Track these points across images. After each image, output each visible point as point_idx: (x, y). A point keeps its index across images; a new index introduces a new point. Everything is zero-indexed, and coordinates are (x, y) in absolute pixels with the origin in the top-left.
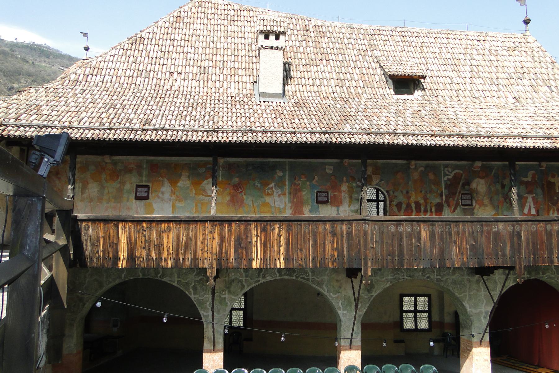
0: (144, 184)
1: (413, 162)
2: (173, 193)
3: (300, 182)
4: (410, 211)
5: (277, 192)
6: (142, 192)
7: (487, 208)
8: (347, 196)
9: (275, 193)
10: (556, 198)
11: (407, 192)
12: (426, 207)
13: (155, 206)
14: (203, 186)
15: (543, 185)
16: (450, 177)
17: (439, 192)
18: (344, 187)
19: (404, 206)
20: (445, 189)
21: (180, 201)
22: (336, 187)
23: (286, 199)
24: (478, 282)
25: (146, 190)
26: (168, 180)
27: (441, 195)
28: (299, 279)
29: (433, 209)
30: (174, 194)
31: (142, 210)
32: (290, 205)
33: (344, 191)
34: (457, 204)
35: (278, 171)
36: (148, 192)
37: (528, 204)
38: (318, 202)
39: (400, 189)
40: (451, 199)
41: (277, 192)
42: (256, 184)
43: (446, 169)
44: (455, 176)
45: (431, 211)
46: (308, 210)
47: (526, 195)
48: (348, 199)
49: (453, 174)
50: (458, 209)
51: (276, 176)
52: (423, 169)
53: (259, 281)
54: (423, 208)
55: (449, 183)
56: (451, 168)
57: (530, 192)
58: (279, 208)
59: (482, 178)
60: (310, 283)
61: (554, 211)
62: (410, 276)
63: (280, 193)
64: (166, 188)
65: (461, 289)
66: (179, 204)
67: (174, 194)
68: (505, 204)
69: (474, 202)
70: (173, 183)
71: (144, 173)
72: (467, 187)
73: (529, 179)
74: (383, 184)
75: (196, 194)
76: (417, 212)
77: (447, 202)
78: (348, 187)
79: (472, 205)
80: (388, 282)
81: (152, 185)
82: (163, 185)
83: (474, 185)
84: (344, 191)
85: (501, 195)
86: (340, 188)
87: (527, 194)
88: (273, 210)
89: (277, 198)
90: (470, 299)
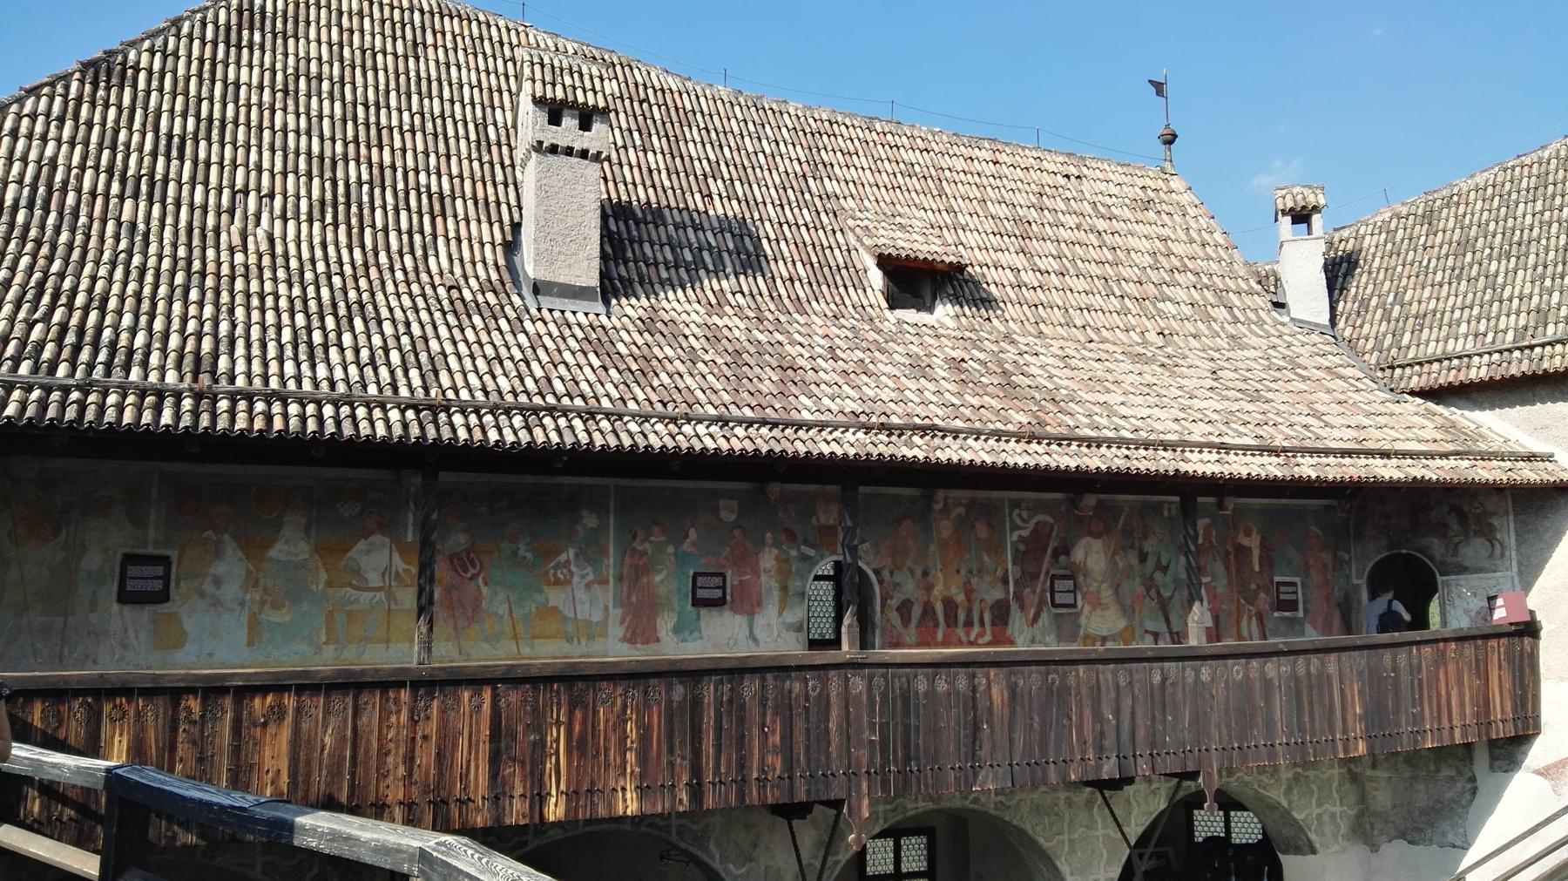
0: (151, 550)
1: (941, 494)
2: (252, 582)
3: (647, 545)
4: (931, 624)
5: (583, 577)
6: (144, 579)
8: (773, 583)
9: (576, 579)
10: (1253, 586)
11: (925, 574)
12: (969, 611)
13: (189, 624)
14: (354, 560)
15: (1227, 553)
16: (1025, 533)
17: (1000, 573)
18: (768, 560)
19: (917, 611)
20: (1014, 563)
21: (277, 605)
22: (745, 559)
23: (607, 595)
24: (1089, 803)
25: (160, 570)
26: (235, 538)
27: (1005, 581)
28: (643, 829)
29: (987, 617)
30: (256, 584)
31: (143, 636)
32: (619, 611)
33: (766, 572)
34: (1042, 602)
35: (584, 513)
36: (166, 579)
38: (698, 603)
39: (909, 563)
40: (1028, 590)
41: (580, 575)
42: (522, 552)
43: (1017, 511)
44: (1035, 531)
45: (982, 624)
46: (670, 625)
48: (776, 593)
49: (1031, 525)
50: (1044, 615)
51: (579, 528)
52: (961, 510)
53: (525, 843)
54: (962, 616)
55: (1022, 547)
56: (1027, 509)
58: (589, 623)
59: (1096, 536)
60: (674, 838)
61: (1250, 618)
62: (932, 800)
63: (591, 577)
64: (231, 566)
65: (1051, 826)
66: (272, 616)
67: (256, 584)
68: (1147, 600)
69: (1079, 597)
70: (254, 548)
71: (153, 517)
72: (1062, 558)
74: (866, 552)
75: (329, 584)
76: (948, 626)
77: (1018, 596)
78: (777, 558)
79: (1074, 606)
80: (877, 820)
81: (181, 556)
82: (218, 555)
83: (1078, 555)
84: (766, 572)
86: (757, 561)
88: (570, 628)
89: (581, 595)
90: (1072, 851)
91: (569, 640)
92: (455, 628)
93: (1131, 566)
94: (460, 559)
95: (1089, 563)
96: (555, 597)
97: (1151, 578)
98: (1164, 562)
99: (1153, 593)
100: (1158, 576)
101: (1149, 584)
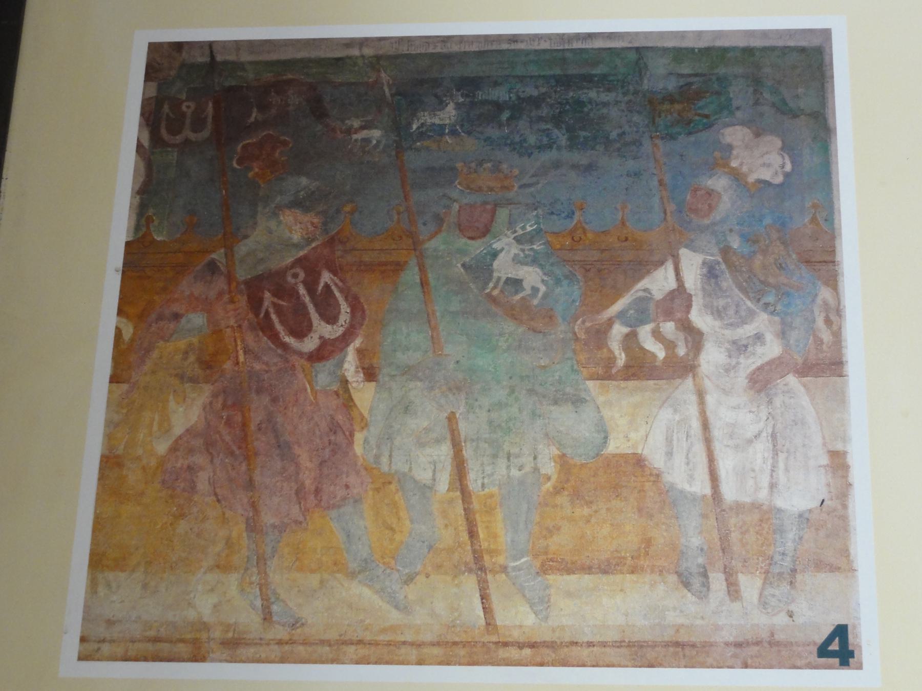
5: (740, 348)
9: (712, 357)
58: (766, 517)
63: (772, 349)
89: (733, 411)
91: (690, 580)
92: (253, 527)
94: (283, 291)
96: (645, 426)
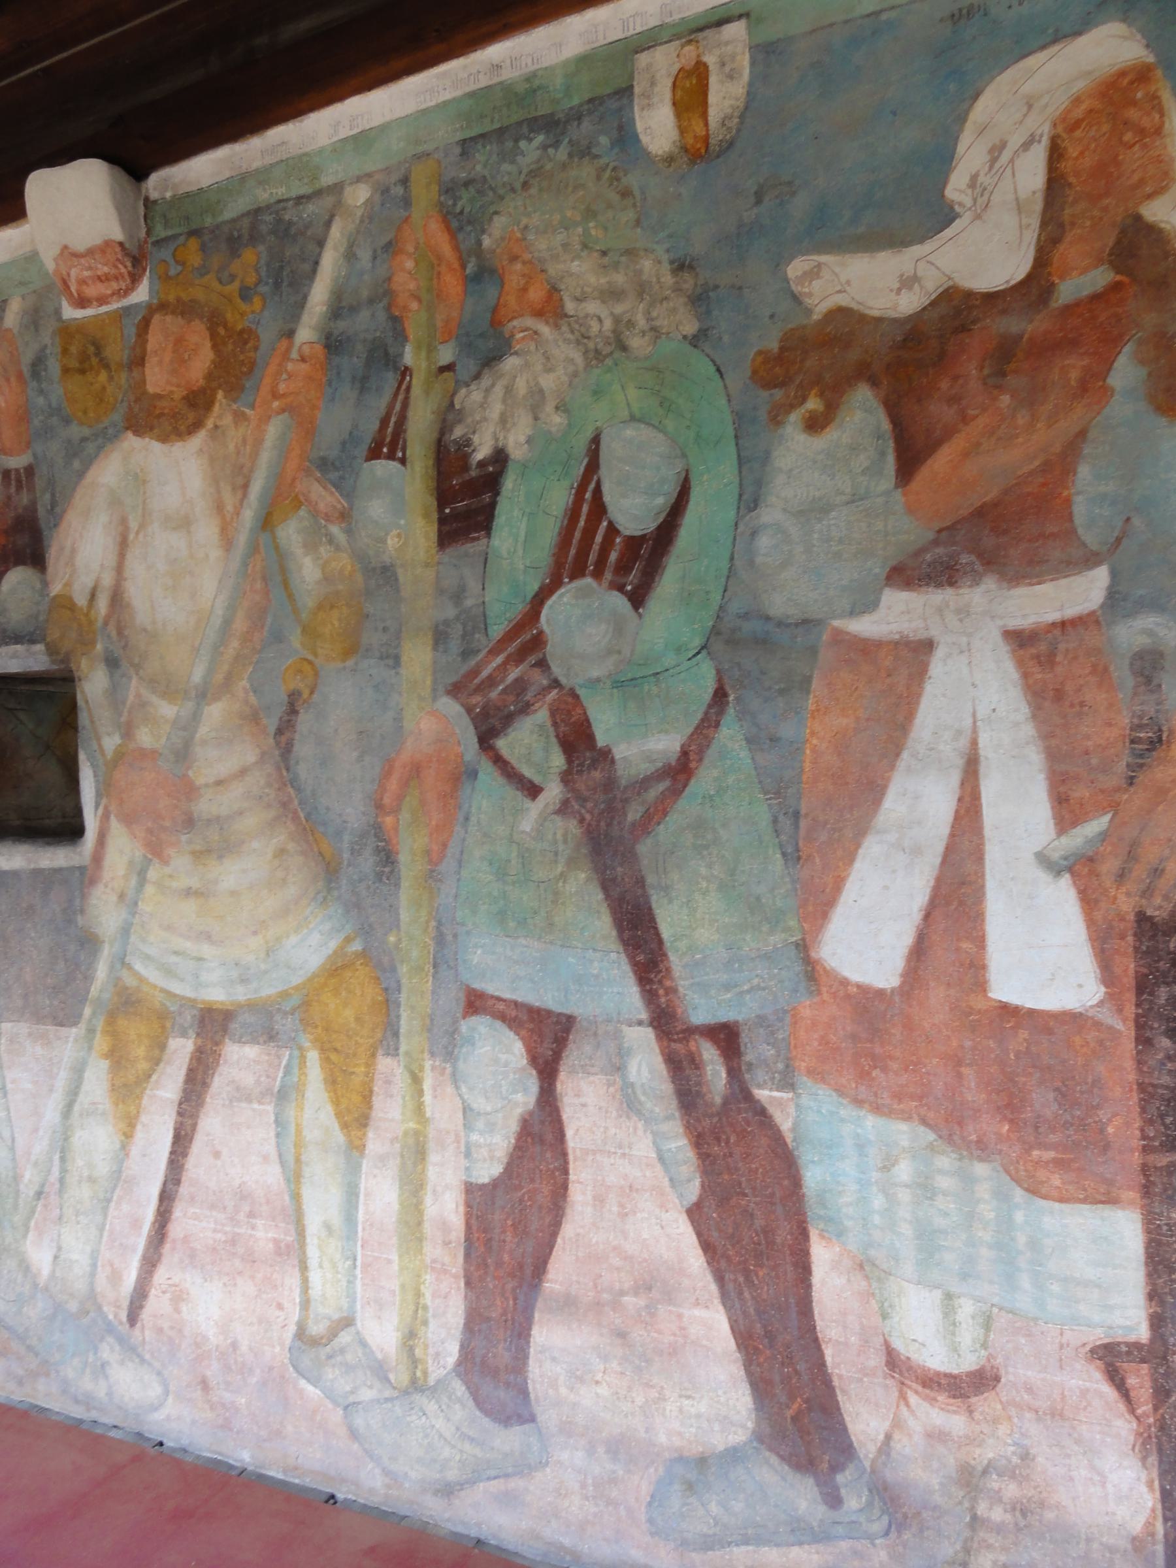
7: (231, 874)
37: (918, 802)
47: (897, 614)
57: (998, 535)
68: (488, 793)
73: (988, 250)
85: (418, 658)
87: (923, 570)
93: (383, 575)
95: (135, 593)
97: (526, 639)
98: (632, 510)
99: (530, 741)
100: (582, 621)
101: (505, 678)
